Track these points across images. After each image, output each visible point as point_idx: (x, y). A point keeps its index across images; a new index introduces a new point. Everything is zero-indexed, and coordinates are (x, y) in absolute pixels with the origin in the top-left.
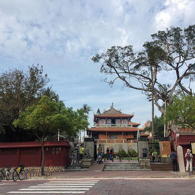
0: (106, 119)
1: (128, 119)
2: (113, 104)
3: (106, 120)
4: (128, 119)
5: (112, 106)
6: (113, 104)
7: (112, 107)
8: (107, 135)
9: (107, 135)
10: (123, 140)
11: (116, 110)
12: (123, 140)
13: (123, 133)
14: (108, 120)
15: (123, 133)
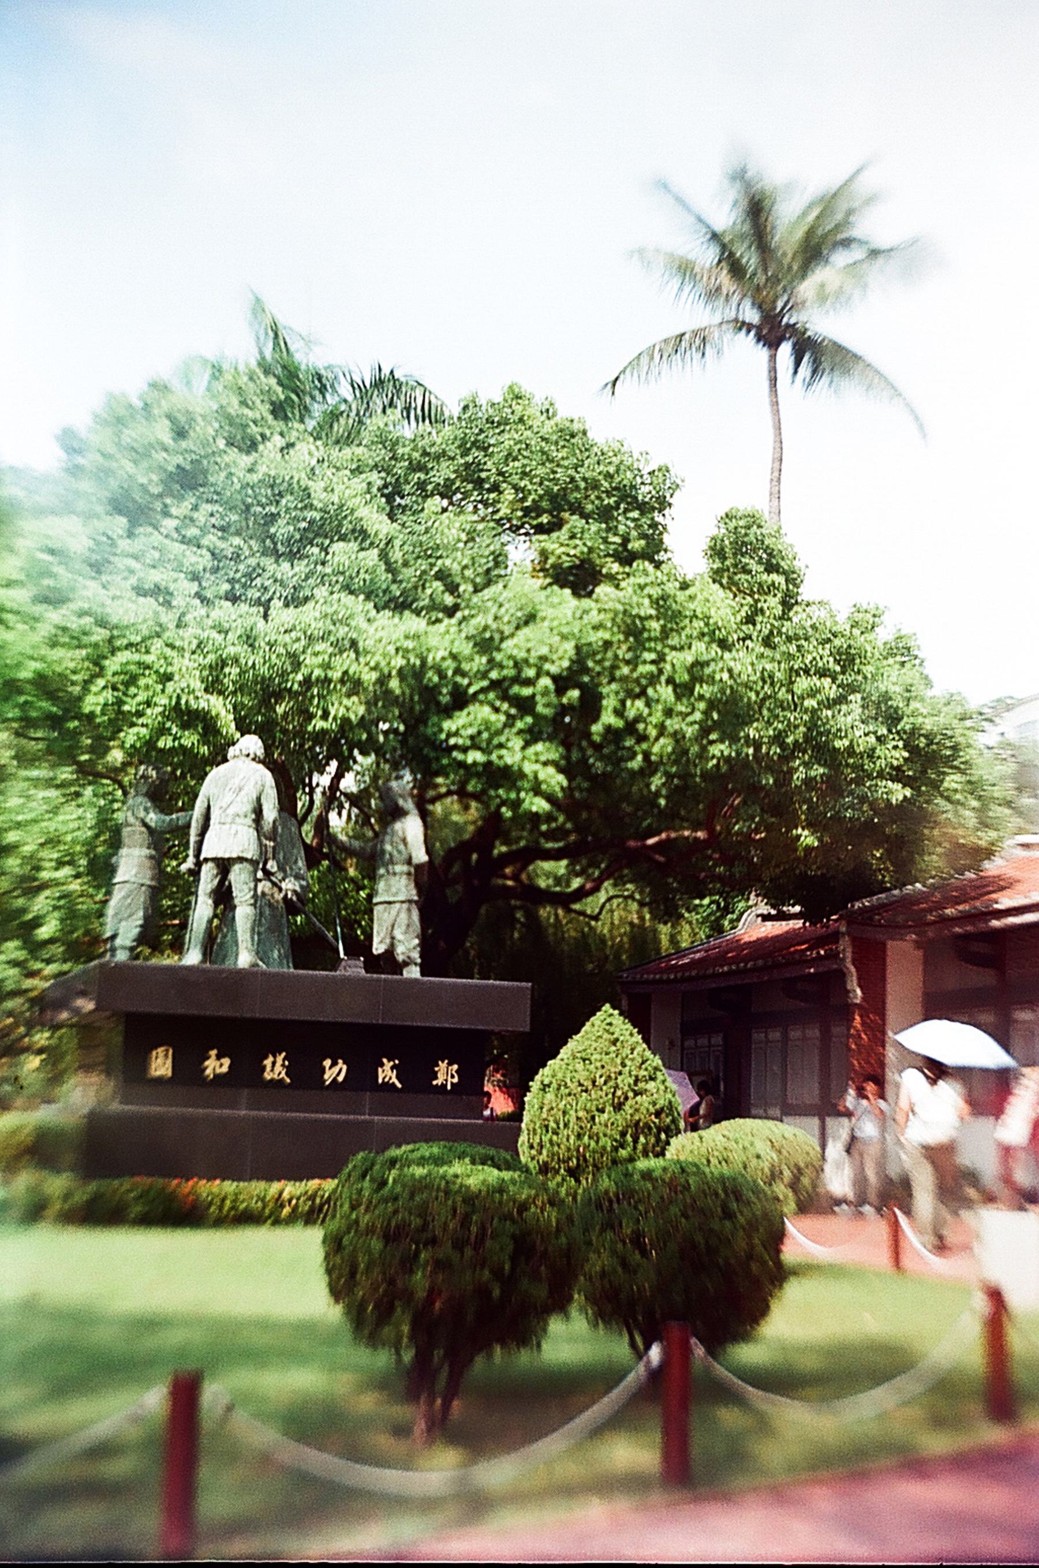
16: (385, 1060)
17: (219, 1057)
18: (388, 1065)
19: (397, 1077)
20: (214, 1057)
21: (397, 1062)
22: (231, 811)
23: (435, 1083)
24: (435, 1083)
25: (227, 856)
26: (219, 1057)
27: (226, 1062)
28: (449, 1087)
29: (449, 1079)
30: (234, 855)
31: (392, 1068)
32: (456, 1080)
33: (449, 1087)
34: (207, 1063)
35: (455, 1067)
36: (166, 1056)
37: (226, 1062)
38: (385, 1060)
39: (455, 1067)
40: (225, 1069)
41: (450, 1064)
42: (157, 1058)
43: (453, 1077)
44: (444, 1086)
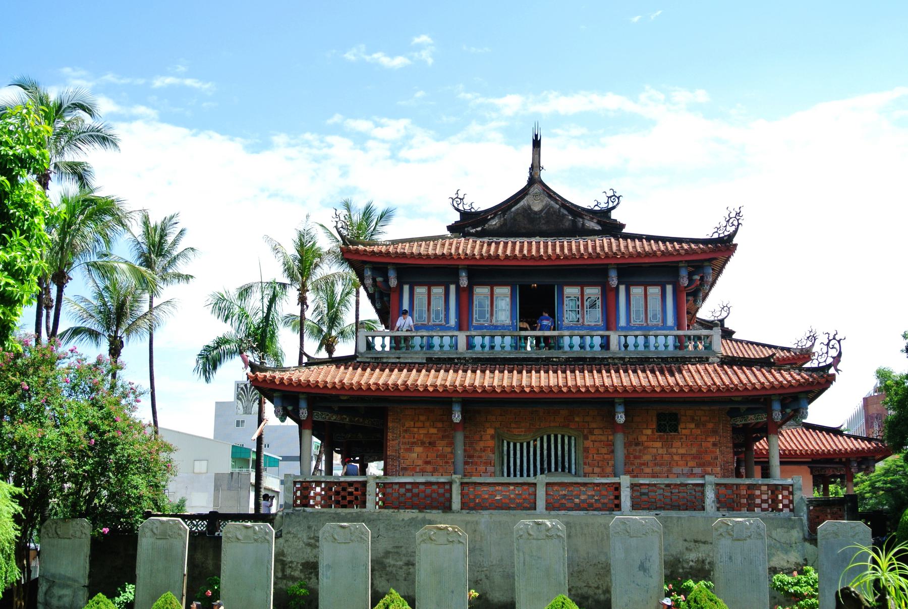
0: (464, 282)
1: (685, 282)
2: (537, 143)
3: (470, 290)
4: (685, 282)
5: (535, 167)
6: (537, 143)
7: (534, 179)
8: (459, 437)
9: (459, 437)
10: (617, 487)
11: (565, 205)
12: (625, 481)
13: (621, 418)
14: (481, 292)
15: (621, 418)
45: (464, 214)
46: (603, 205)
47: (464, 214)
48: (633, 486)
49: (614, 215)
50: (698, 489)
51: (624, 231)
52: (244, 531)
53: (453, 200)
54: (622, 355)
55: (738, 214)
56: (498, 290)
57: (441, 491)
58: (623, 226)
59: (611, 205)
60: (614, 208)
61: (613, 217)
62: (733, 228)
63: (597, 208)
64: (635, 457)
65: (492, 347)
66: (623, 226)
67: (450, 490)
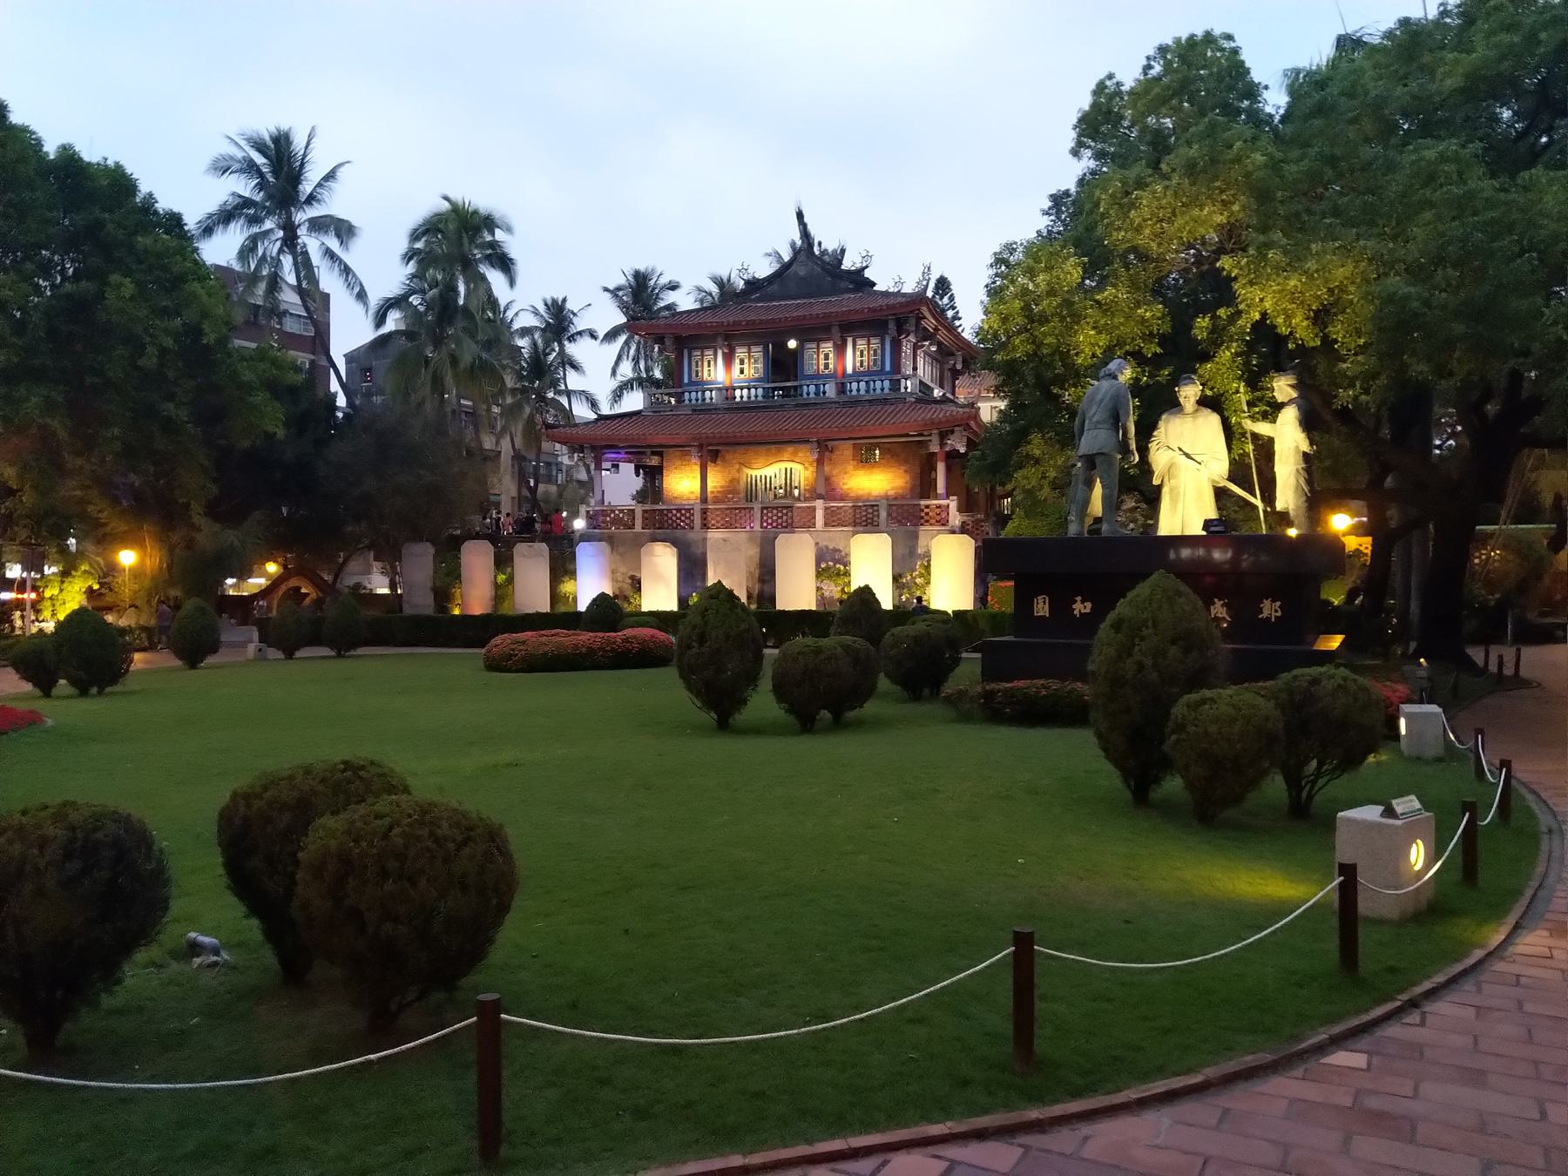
2: (800, 215)
6: (800, 215)
10: (814, 509)
16: (1216, 600)
17: (1083, 602)
18: (1218, 603)
19: (1226, 613)
20: (1079, 602)
21: (1226, 601)
22: (1094, 420)
23: (1260, 616)
24: (1260, 616)
25: (1090, 453)
26: (1083, 602)
27: (1089, 605)
28: (1273, 620)
29: (1273, 614)
30: (1094, 452)
31: (1222, 606)
32: (1279, 614)
33: (1273, 620)
34: (1074, 606)
35: (1278, 603)
36: (1044, 602)
37: (1089, 605)
38: (1216, 600)
39: (1278, 603)
40: (1088, 610)
41: (1273, 601)
42: (1038, 603)
43: (1276, 611)
44: (1268, 619)
45: (747, 282)
46: (858, 265)
47: (747, 282)
48: (826, 508)
49: (867, 273)
50: (875, 508)
51: (875, 288)
52: (527, 548)
53: (740, 271)
54: (837, 400)
55: (929, 268)
56: (754, 349)
57: (688, 515)
58: (874, 284)
59: (864, 265)
60: (867, 267)
61: (866, 276)
62: (924, 283)
63: (853, 268)
64: (844, 484)
65: (704, 400)
66: (874, 284)
67: (693, 515)
